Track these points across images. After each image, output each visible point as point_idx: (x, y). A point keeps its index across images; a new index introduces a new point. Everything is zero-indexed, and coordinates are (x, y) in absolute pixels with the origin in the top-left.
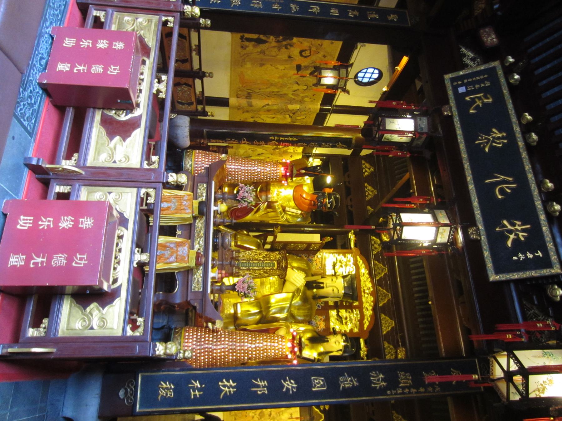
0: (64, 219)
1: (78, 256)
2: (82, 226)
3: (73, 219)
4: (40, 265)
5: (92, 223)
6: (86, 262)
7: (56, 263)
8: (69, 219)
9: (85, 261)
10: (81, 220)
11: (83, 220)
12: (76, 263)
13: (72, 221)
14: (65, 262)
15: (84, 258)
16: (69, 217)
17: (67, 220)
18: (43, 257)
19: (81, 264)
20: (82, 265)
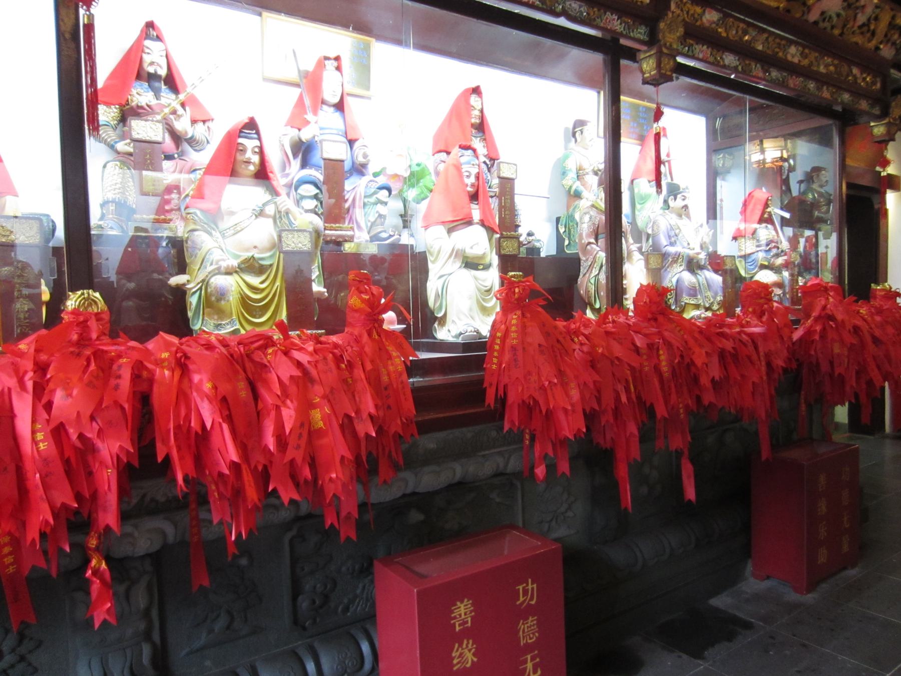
0: (458, 663)
1: (522, 599)
2: (469, 619)
3: (457, 645)
4: (538, 660)
5: (462, 602)
6: (530, 581)
7: (533, 634)
8: (458, 654)
9: (527, 585)
10: (457, 628)
11: (457, 624)
12: (532, 599)
13: (461, 645)
14: (530, 619)
15: (523, 588)
16: (454, 655)
17: (461, 654)
18: (525, 662)
19: (533, 589)
20: (535, 586)
